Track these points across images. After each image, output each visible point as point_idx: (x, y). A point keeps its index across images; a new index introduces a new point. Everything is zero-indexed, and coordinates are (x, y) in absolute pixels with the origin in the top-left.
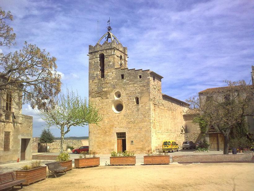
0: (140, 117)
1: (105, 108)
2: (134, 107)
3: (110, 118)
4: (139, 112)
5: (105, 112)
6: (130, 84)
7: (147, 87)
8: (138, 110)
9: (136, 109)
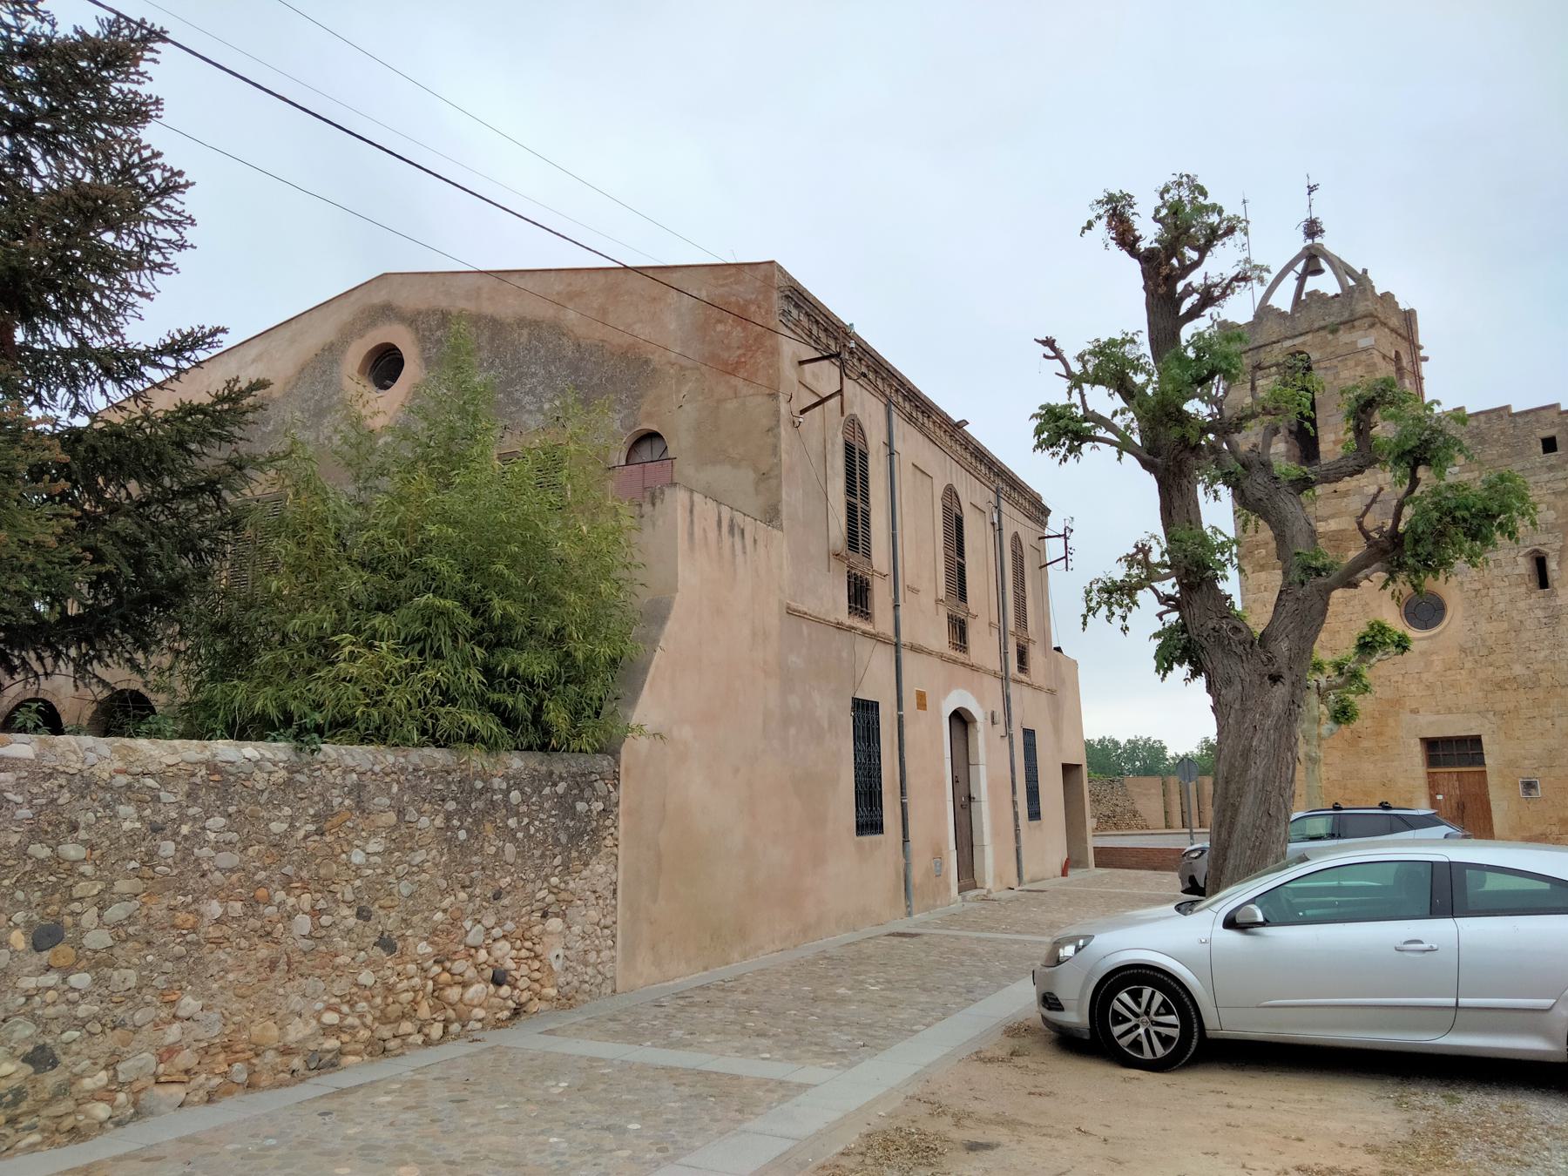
2: (1522, 605)
9: (1540, 613)
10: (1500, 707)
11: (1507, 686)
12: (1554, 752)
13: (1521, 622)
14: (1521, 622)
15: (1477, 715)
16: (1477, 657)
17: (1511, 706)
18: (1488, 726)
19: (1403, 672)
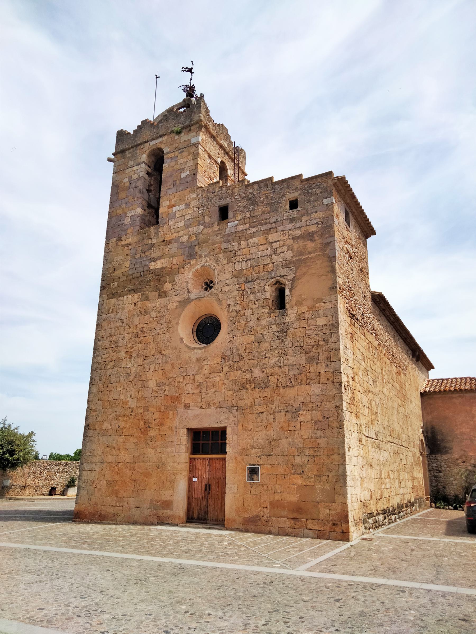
0: (291, 359)
1: (150, 330)
2: (264, 322)
3: (168, 367)
4: (288, 341)
5: (153, 345)
6: (252, 236)
7: (321, 237)
8: (283, 332)
9: (275, 328)
10: (241, 404)
11: (248, 386)
12: (273, 443)
13: (263, 335)
14: (263, 335)
15: (225, 409)
16: (232, 363)
17: (248, 402)
18: (232, 418)
19: (184, 374)
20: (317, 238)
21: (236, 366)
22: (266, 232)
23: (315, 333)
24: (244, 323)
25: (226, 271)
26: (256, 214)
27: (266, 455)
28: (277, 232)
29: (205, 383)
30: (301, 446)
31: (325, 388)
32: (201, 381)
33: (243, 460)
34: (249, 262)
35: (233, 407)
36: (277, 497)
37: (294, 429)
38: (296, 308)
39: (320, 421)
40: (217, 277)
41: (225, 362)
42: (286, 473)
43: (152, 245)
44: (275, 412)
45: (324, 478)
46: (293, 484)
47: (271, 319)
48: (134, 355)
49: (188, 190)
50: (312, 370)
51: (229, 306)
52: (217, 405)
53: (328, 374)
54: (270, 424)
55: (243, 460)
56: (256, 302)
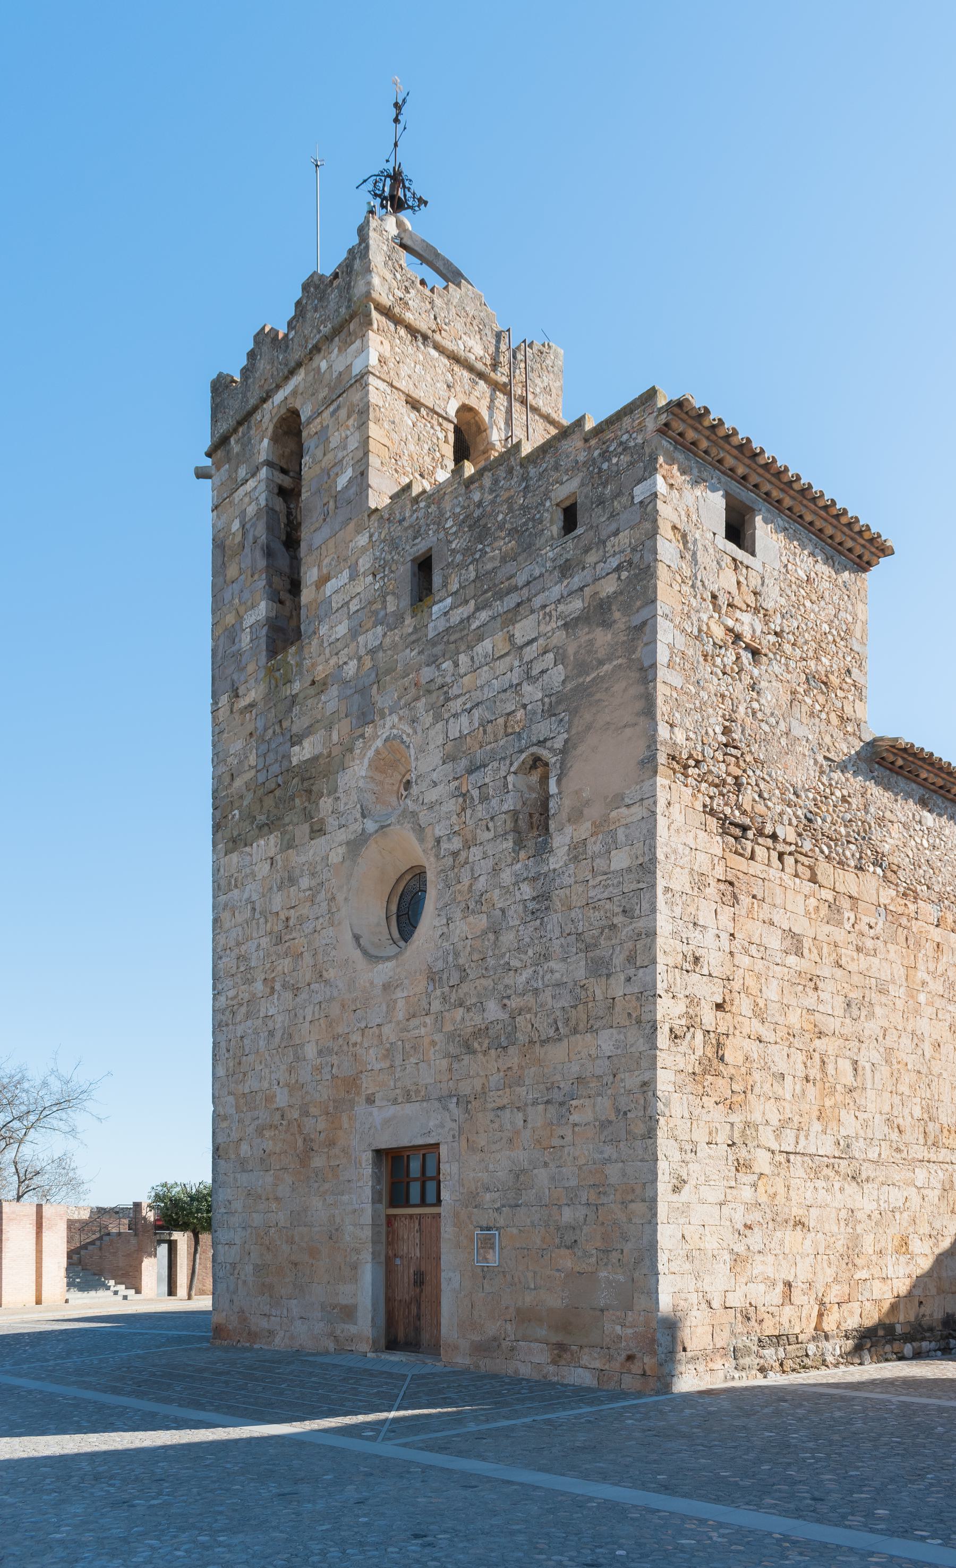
1: (301, 920)
2: (506, 877)
3: (335, 1010)
4: (554, 919)
5: (308, 959)
7: (627, 609)
10: (465, 1088)
11: (476, 1045)
12: (522, 1178)
14: (503, 911)
16: (446, 989)
17: (478, 1083)
18: (450, 1124)
19: (363, 1025)
20: (617, 615)
21: (454, 997)
22: (510, 615)
23: (606, 895)
24: (468, 884)
25: (432, 746)
26: (489, 566)
27: (510, 1206)
28: (532, 612)
29: (400, 1043)
30: (573, 1183)
31: (623, 1038)
32: (393, 1039)
33: (469, 1218)
34: (476, 713)
35: (450, 1096)
36: (528, 1299)
37: (561, 1142)
38: (569, 829)
39: (610, 1122)
40: (414, 766)
41: (435, 989)
42: (545, 1247)
43: (294, 699)
44: (526, 1105)
45: (615, 1256)
46: (558, 1270)
47: (519, 866)
48: (278, 986)
49: (352, 525)
50: (598, 993)
51: (438, 841)
52: (423, 1093)
53: (630, 1001)
54: (517, 1133)
55: (469, 1218)
56: (491, 825)
